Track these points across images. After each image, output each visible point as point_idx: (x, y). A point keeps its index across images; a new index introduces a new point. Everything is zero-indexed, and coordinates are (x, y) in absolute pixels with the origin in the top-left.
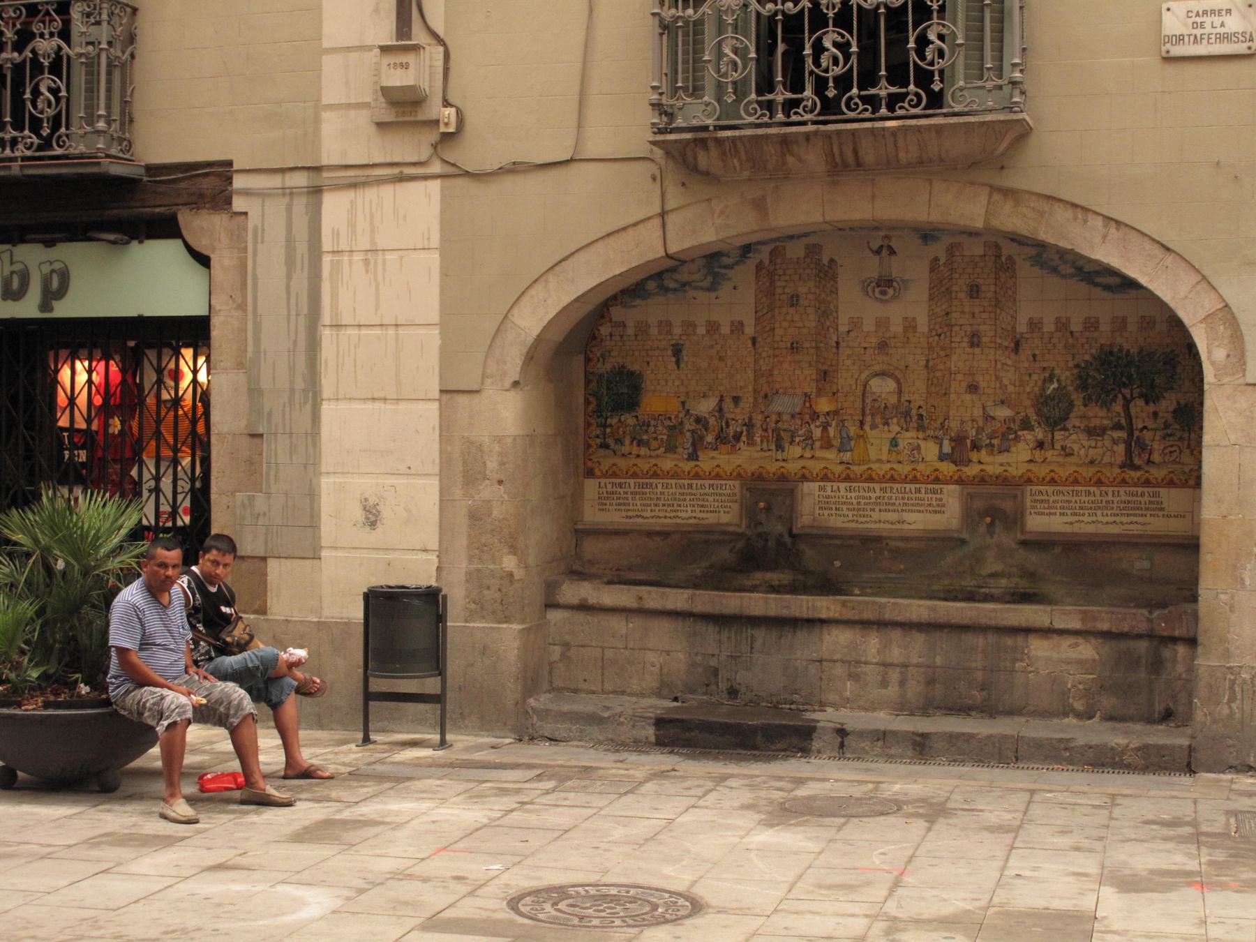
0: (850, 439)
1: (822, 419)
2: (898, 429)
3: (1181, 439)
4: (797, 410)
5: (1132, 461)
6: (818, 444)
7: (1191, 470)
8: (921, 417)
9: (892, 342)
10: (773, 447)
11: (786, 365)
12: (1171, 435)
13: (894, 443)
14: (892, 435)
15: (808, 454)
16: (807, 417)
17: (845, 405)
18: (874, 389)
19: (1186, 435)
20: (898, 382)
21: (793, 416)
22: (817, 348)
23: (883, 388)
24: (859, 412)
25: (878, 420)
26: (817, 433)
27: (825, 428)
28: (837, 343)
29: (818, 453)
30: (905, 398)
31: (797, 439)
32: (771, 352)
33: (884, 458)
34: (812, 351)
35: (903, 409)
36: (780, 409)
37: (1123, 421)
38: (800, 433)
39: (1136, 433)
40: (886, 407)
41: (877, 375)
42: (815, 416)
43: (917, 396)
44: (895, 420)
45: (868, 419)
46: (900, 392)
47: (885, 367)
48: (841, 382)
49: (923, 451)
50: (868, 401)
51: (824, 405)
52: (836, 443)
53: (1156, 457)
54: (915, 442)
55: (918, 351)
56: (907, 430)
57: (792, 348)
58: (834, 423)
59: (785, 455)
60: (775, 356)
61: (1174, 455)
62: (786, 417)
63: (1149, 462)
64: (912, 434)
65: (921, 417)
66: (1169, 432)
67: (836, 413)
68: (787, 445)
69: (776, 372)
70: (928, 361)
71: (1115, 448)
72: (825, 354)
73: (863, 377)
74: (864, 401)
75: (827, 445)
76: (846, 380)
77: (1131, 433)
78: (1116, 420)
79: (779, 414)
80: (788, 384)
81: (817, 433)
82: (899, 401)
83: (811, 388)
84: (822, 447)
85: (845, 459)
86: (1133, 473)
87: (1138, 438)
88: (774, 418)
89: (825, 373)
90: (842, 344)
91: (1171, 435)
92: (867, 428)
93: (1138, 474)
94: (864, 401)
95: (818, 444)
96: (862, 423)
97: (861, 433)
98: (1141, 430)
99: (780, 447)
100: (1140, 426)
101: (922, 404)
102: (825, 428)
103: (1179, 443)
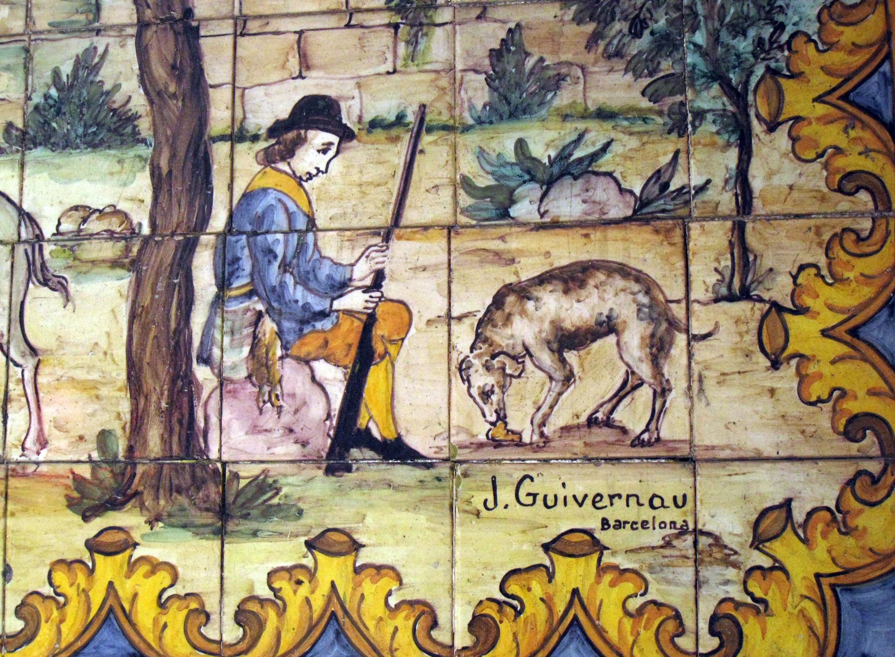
3: (660, 207)
5: (187, 433)
7: (773, 522)
12: (567, 168)
19: (708, 165)
37: (121, 71)
39: (238, 170)
53: (420, 397)
61: (597, 376)
63: (350, 441)
66: (543, 141)
71: (44, 311)
77: (186, 173)
78: (62, 56)
86: (191, 557)
87: (248, 220)
91: (567, 168)
93: (254, 561)
98: (286, 135)
100: (273, 104)
103: (641, 250)
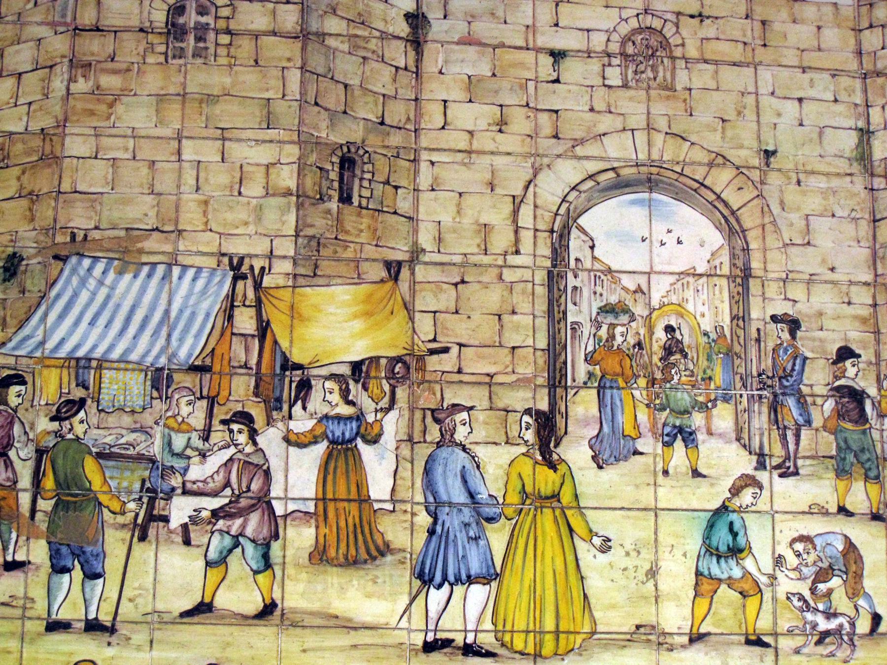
0: (483, 515)
1: (325, 399)
2: (745, 464)
4: (188, 349)
6: (300, 538)
8: (852, 399)
9: (690, 39)
10: (38, 552)
11: (136, 115)
13: (722, 538)
14: (711, 496)
15: (240, 594)
16: (241, 388)
17: (458, 329)
18: (611, 254)
20: (731, 225)
21: (160, 380)
22: (304, 36)
23: (655, 253)
24: (531, 366)
25: (635, 410)
26: (298, 476)
27: (342, 451)
28: (417, 20)
29: (300, 592)
30: (757, 312)
31: (180, 510)
32: (59, 45)
33: (675, 617)
34: (281, 50)
35: (759, 361)
36: (87, 340)
38: (197, 472)
40: (673, 348)
41: (621, 186)
42: (286, 382)
43: (823, 299)
44: (724, 418)
45: (583, 406)
46: (743, 278)
47: (667, 150)
48: (435, 210)
49: (868, 584)
50: (581, 312)
51: (335, 327)
52: (405, 533)
54: (832, 532)
55: (822, 87)
56: (787, 471)
57: (175, 30)
58: (392, 426)
59: (102, 600)
60: (80, 66)
62: (124, 387)
64: (815, 488)
65: (852, 399)
67: (404, 368)
68: (115, 543)
69: (76, 145)
70: (865, 134)
72: (348, 68)
73: (552, 188)
74: (555, 314)
75: (353, 543)
76: (455, 203)
79: (81, 367)
80: (141, 211)
81: (298, 476)
82: (740, 318)
83: (265, 231)
84: (320, 556)
85: (451, 625)
88: (51, 385)
89: (347, 163)
90: (438, 28)
92: (575, 452)
94: (555, 314)
95: (300, 538)
96: (548, 429)
97: (547, 481)
99: (75, 554)
101: (856, 337)
102: (342, 451)
